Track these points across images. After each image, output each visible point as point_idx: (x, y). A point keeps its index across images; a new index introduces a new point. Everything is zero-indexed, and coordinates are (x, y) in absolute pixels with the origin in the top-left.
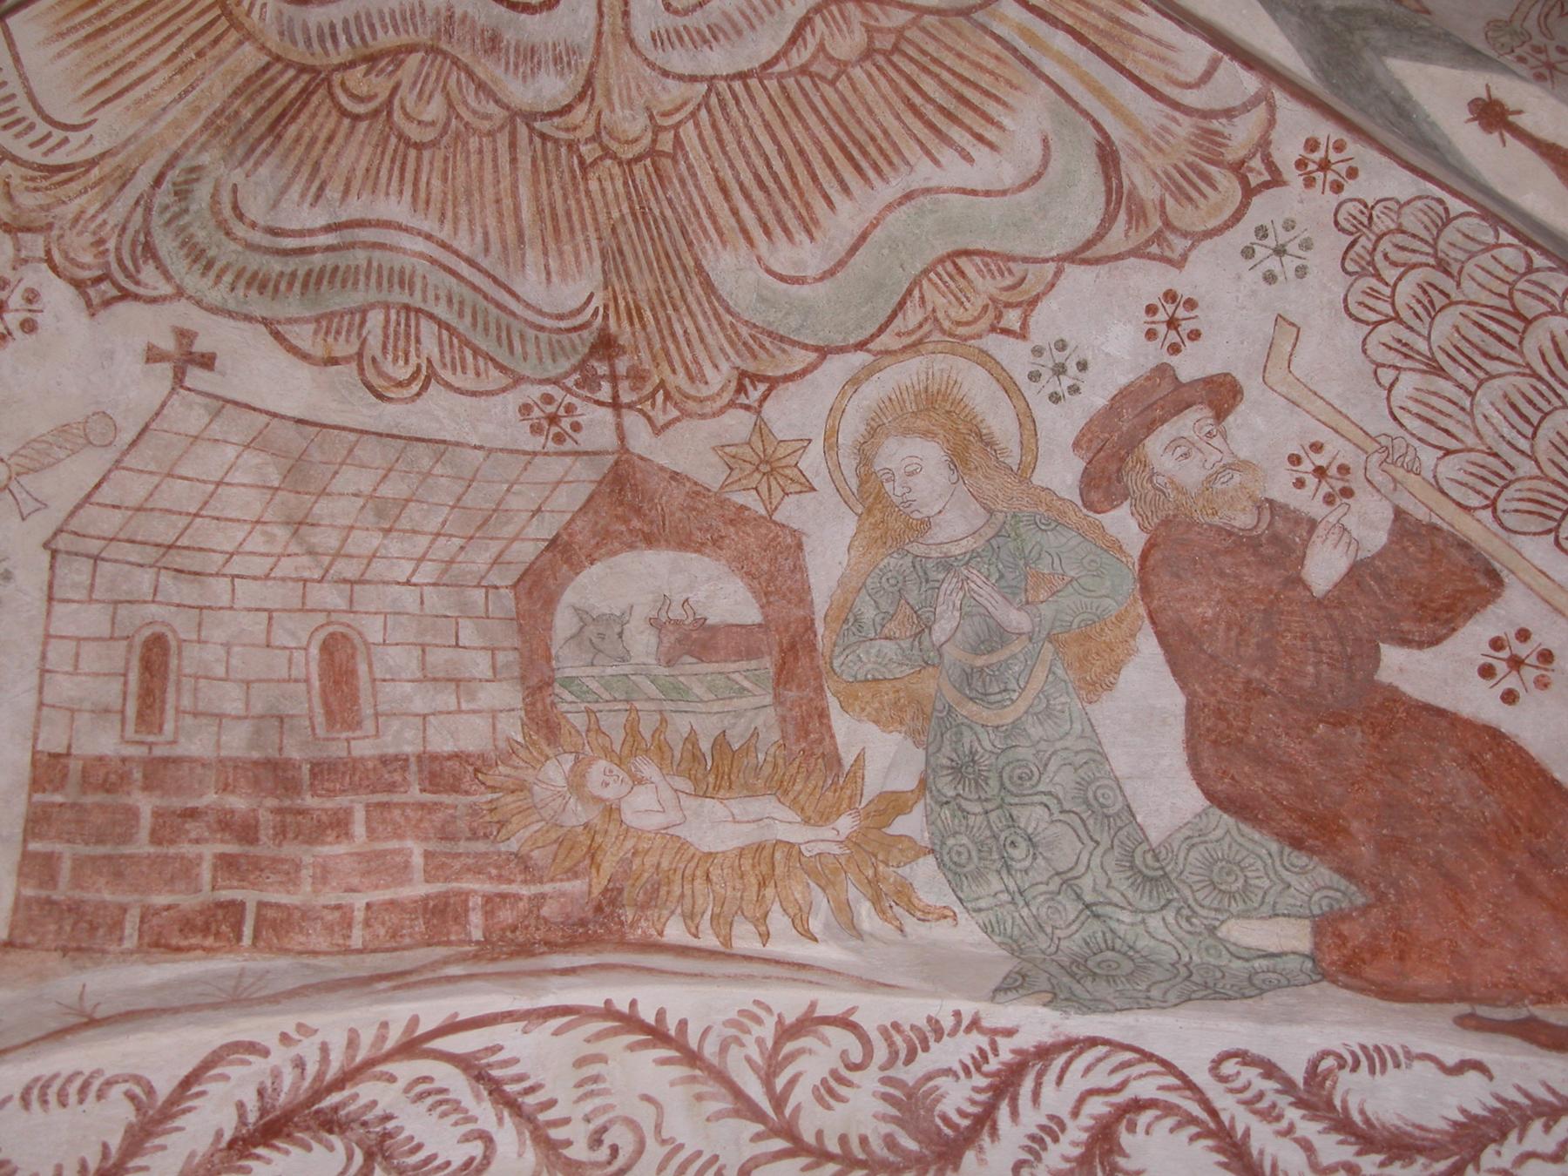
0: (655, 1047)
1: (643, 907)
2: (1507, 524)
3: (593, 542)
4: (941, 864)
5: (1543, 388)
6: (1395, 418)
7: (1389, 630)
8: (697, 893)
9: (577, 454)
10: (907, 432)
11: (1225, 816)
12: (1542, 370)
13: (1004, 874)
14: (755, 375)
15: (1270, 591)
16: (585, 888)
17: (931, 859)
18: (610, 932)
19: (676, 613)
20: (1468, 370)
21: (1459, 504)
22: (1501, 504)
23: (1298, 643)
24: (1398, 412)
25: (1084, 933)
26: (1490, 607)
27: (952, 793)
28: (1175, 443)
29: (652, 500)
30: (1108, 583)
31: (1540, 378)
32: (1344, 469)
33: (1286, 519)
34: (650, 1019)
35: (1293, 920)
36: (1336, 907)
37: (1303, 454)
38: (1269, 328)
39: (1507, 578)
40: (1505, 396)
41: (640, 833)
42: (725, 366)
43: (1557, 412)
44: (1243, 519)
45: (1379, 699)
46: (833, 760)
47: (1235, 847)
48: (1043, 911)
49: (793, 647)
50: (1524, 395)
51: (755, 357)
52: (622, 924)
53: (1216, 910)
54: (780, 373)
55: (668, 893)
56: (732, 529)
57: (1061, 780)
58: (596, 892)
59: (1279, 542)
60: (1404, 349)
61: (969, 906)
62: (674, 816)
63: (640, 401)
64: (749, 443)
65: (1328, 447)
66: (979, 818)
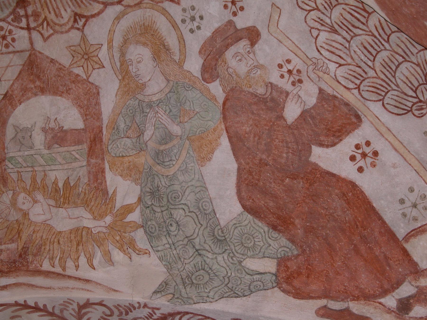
0: (37, 312)
1: (35, 255)
2: (365, 96)
3: (21, 94)
4: (145, 232)
5: (377, 41)
6: (319, 51)
7: (316, 140)
8: (55, 249)
9: (14, 52)
10: (138, 42)
11: (249, 215)
12: (376, 34)
13: (168, 238)
14: (80, 15)
15: (271, 121)
16: (16, 247)
17: (142, 229)
18: (23, 265)
19: (52, 125)
20: (347, 32)
21: (345, 87)
22: (362, 88)
23: (281, 144)
24: (319, 48)
25: (194, 262)
26: (356, 130)
27: (150, 203)
28: (236, 54)
29: (44, 72)
30: (211, 115)
31: (375, 37)
32: (299, 71)
33: (277, 91)
34: (33, 305)
35: (270, 259)
36: (286, 255)
37: (283, 64)
38: (269, 8)
39: (364, 119)
40: (362, 44)
41: (36, 224)
42: (69, 10)
43: (383, 51)
44: (261, 91)
45: (310, 169)
46: (105, 192)
47: (252, 228)
48: (181, 251)
49: (95, 139)
50: (369, 44)
51: (80, 6)
52: (28, 262)
53: (242, 254)
54: (89, 14)
55: (45, 249)
56: (74, 85)
57: (189, 198)
58: (20, 248)
59: (273, 101)
60: (321, 22)
61: (155, 249)
62: (48, 216)
63: (38, 26)
64: (79, 45)
65: (293, 62)
66: (160, 214)
